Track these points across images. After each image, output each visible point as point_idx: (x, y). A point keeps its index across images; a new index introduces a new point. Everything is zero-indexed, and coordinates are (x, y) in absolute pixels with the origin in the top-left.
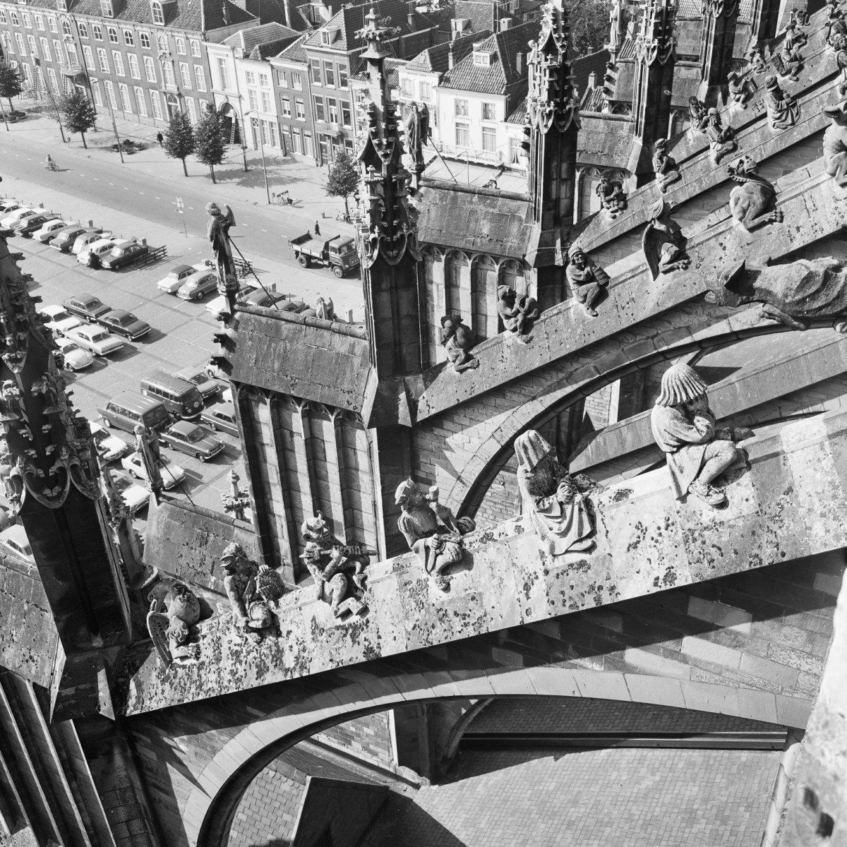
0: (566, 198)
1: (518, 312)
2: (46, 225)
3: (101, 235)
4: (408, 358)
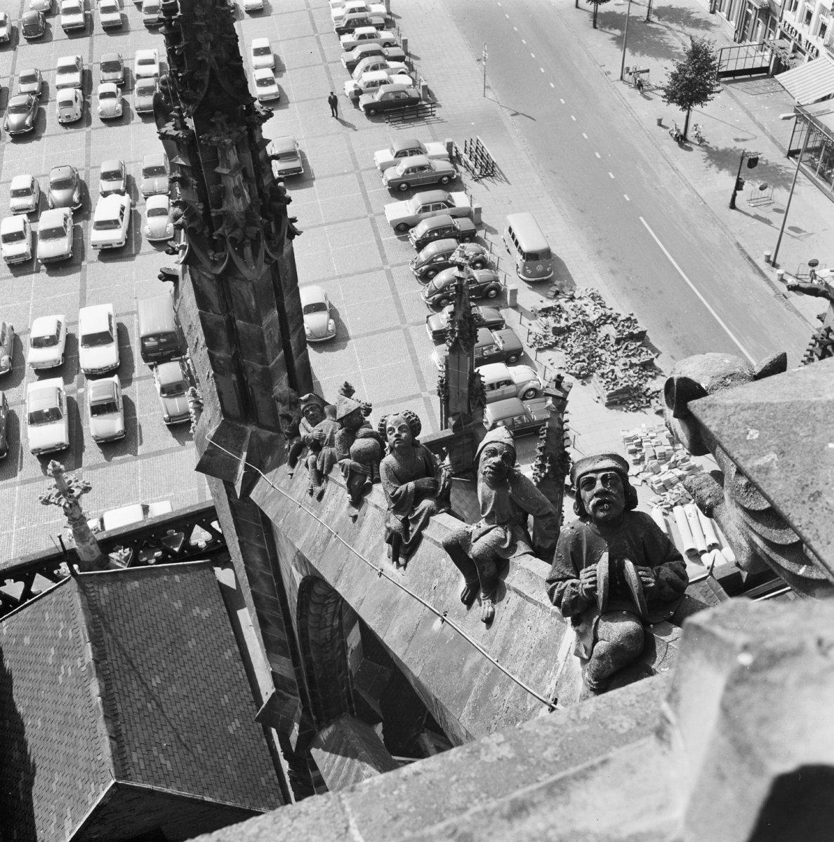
2: (360, 31)
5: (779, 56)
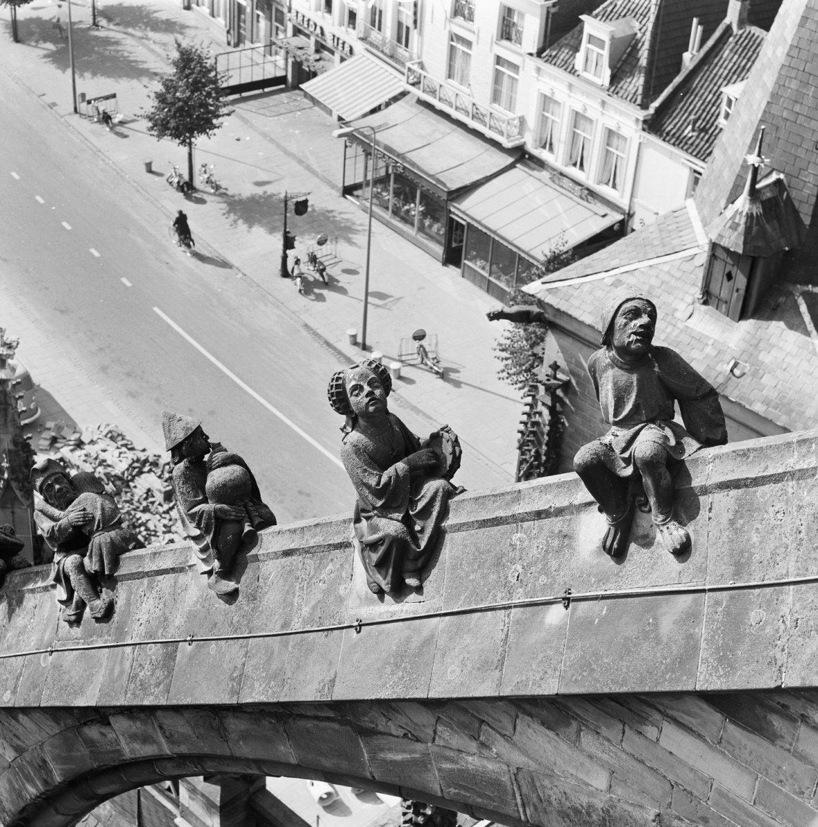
5: (298, 60)
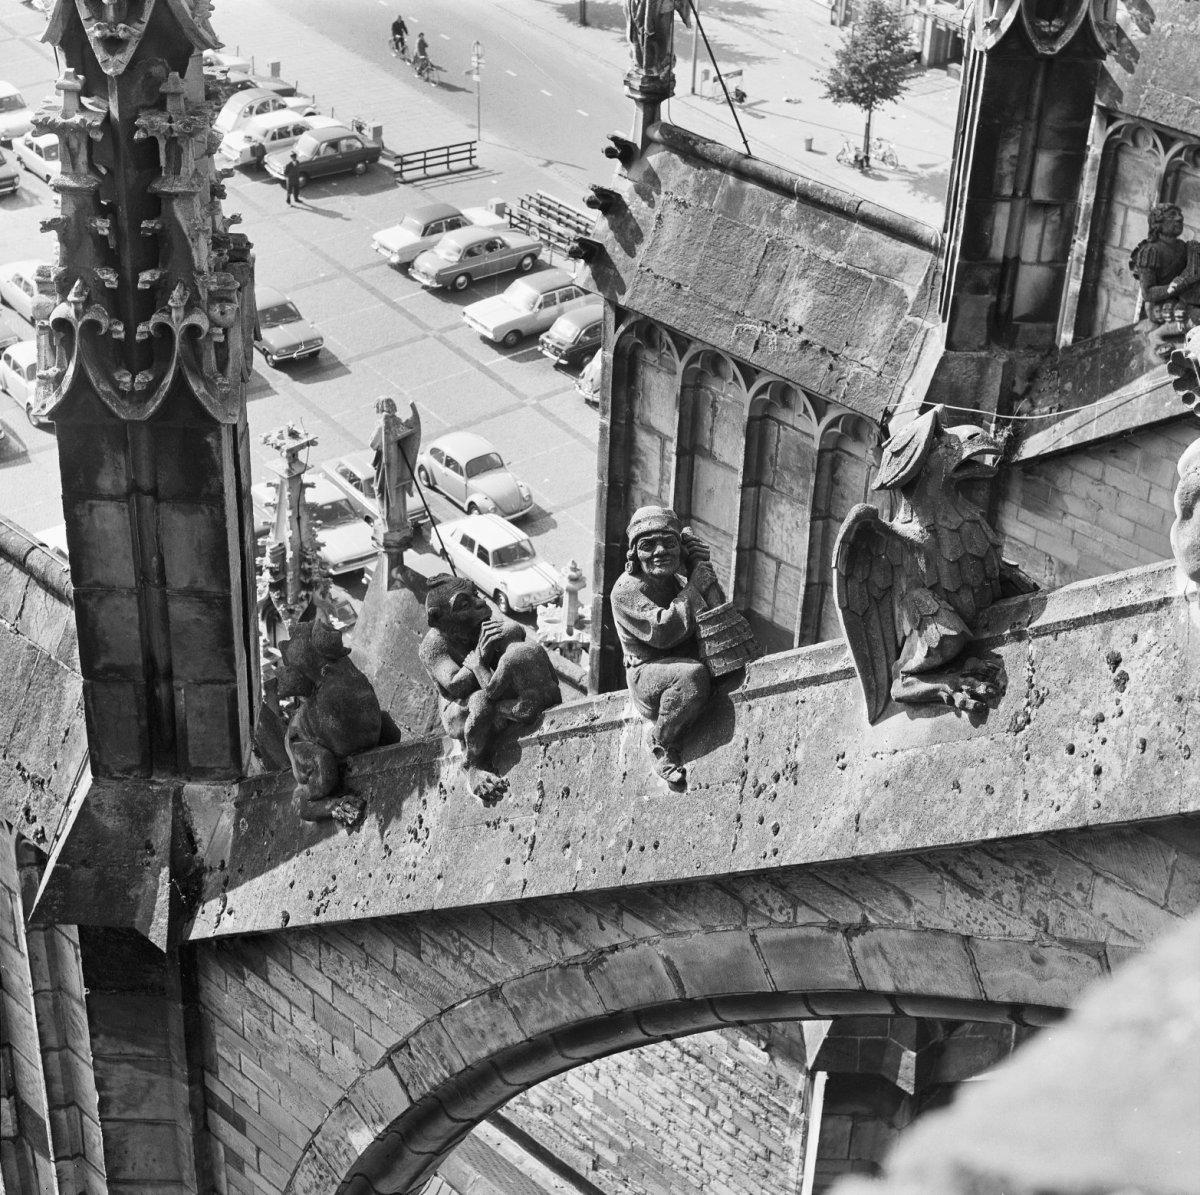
0: (1039, 262)
1: (471, 684)
3: (288, 100)
4: (194, 727)
5: (952, 28)
